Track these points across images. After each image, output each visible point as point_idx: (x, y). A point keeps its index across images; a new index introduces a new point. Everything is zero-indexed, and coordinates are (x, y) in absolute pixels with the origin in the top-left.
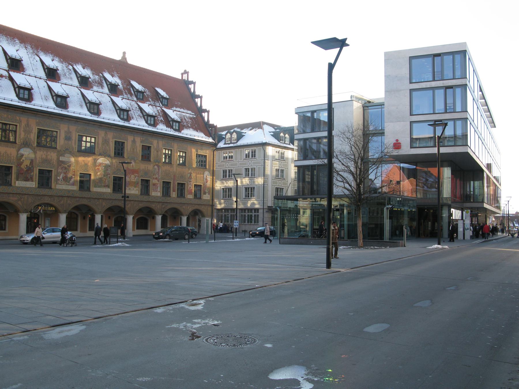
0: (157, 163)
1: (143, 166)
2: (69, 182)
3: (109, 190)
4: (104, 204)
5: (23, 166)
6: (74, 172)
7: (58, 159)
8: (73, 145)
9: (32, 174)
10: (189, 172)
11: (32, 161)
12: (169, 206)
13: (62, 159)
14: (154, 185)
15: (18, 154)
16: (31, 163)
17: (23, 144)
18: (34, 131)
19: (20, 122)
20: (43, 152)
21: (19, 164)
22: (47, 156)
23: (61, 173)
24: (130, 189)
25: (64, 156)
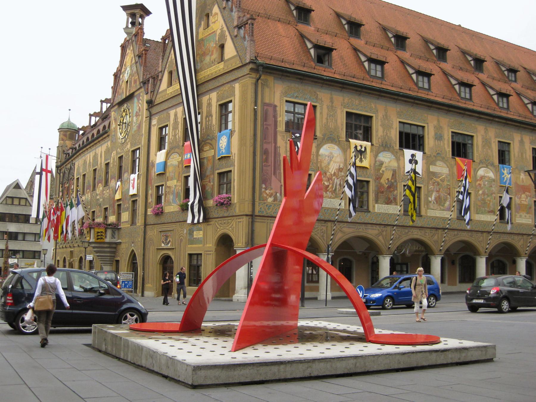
2: (443, 206)
6: (449, 189)
7: (428, 169)
8: (446, 146)
9: (396, 191)
15: (376, 162)
16: (393, 175)
17: (382, 145)
19: (376, 112)
21: (378, 178)
23: (433, 191)
24: (521, 216)
25: (435, 165)
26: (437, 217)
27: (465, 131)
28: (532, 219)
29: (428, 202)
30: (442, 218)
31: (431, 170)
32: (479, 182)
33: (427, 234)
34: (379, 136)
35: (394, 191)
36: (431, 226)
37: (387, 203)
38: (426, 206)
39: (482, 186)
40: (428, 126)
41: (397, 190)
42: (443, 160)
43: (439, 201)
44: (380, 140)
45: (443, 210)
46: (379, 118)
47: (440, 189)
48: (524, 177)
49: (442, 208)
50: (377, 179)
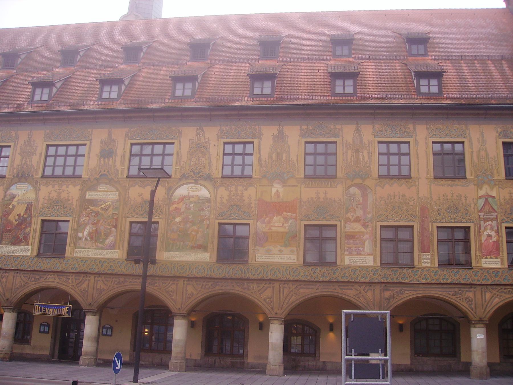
0: (358, 181)
1: (309, 193)
3: (205, 257)
4: (190, 289)
5: (13, 218)
6: (117, 220)
7: (83, 196)
8: (118, 164)
9: (29, 229)
10: (482, 193)
11: (29, 206)
12: (409, 294)
13: (90, 195)
14: (350, 236)
15: (5, 196)
16: (27, 209)
17: (18, 176)
18: (38, 152)
20: (53, 187)
22: (59, 193)
23: (86, 225)
26: (90, 258)
27: (157, 139)
28: (298, 255)
29: (77, 239)
30: (98, 259)
31: (87, 197)
32: (175, 206)
33: (70, 281)
34: (15, 166)
35: (26, 228)
36: (78, 270)
37: (14, 244)
38: (72, 245)
39: (183, 210)
40: (91, 143)
41: (30, 226)
42: (111, 182)
43: (96, 237)
44: (15, 171)
45: (102, 248)
46: (18, 146)
47: (98, 221)
48: (281, 189)
49: (100, 245)
50: (5, 216)
